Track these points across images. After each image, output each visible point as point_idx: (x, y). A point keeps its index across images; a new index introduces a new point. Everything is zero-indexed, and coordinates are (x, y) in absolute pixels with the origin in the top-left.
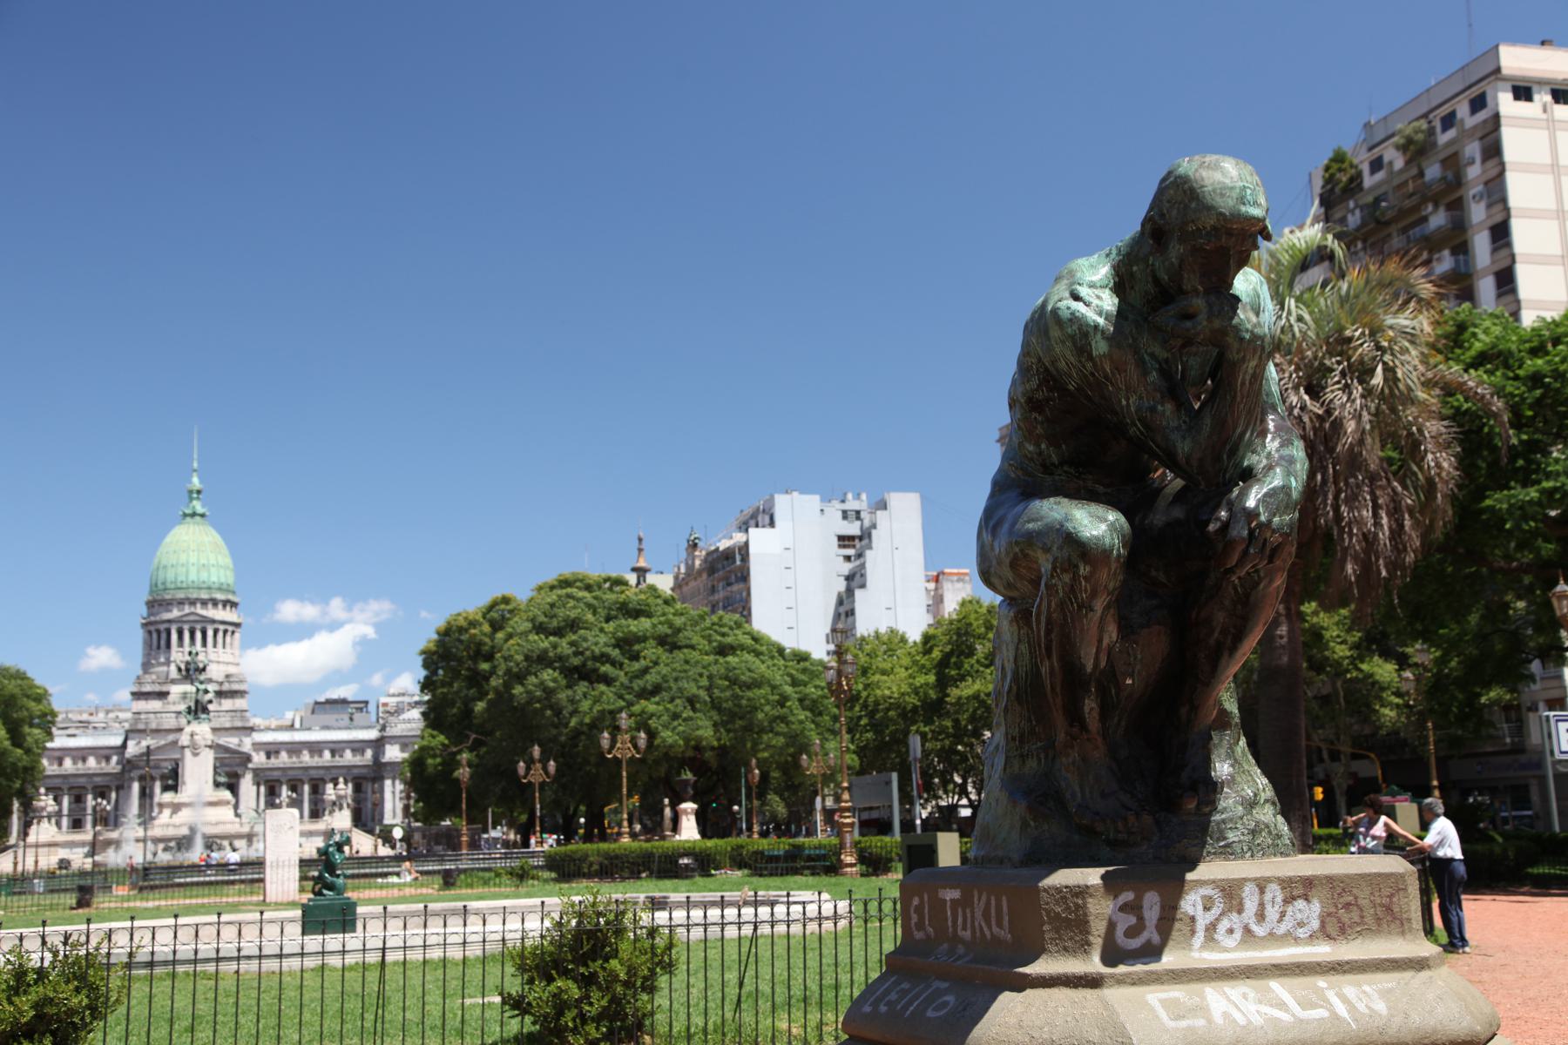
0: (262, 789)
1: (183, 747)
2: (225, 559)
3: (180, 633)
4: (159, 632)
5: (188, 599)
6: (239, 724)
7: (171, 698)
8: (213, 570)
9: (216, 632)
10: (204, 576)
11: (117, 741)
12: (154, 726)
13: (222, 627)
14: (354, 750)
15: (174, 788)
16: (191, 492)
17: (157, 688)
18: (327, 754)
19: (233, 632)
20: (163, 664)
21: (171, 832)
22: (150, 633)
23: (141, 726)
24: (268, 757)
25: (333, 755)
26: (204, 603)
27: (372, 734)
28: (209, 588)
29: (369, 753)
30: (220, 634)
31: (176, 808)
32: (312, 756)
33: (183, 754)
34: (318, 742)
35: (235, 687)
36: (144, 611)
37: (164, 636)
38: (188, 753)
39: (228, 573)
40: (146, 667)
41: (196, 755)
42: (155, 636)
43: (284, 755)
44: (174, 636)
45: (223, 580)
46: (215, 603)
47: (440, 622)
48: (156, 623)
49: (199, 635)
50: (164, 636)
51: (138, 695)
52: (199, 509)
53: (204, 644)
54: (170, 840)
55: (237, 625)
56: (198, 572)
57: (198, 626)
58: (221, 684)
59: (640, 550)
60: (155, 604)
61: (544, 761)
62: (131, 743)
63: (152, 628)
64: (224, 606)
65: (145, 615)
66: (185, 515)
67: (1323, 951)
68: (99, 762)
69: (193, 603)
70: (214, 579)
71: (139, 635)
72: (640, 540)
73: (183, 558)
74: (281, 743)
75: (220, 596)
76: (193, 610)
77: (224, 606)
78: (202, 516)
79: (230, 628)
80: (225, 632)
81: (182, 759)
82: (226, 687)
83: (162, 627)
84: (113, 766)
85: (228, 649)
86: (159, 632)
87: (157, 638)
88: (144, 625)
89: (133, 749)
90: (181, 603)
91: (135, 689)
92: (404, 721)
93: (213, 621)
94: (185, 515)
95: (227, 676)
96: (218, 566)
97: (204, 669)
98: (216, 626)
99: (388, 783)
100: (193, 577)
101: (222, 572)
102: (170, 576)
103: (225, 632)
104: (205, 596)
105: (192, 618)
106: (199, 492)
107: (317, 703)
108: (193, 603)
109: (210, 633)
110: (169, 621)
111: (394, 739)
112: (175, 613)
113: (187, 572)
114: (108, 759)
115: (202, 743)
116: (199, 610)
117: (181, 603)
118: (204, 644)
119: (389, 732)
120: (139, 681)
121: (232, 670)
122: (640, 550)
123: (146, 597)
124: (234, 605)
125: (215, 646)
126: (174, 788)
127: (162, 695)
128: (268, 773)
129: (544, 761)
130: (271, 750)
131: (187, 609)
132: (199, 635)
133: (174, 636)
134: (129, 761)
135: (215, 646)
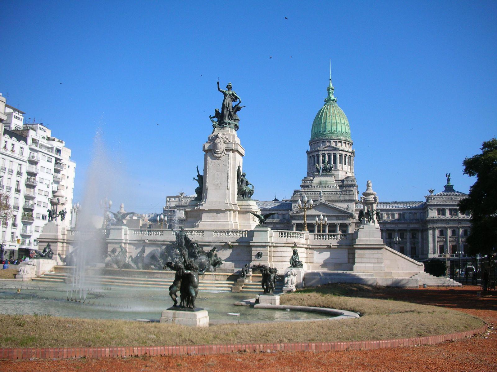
3: (324, 156)
5: (327, 139)
6: (348, 198)
8: (339, 125)
9: (341, 155)
10: (334, 128)
13: (344, 153)
22: (310, 157)
35: (350, 183)
37: (316, 158)
39: (347, 127)
42: (312, 159)
44: (321, 158)
45: (344, 130)
49: (332, 157)
50: (316, 158)
57: (332, 152)
63: (311, 155)
65: (309, 150)
70: (339, 129)
71: (305, 158)
78: (333, 100)
79: (348, 154)
86: (314, 156)
88: (308, 153)
98: (341, 152)
101: (343, 126)
109: (338, 156)
116: (333, 144)
131: (327, 144)
132: (332, 157)
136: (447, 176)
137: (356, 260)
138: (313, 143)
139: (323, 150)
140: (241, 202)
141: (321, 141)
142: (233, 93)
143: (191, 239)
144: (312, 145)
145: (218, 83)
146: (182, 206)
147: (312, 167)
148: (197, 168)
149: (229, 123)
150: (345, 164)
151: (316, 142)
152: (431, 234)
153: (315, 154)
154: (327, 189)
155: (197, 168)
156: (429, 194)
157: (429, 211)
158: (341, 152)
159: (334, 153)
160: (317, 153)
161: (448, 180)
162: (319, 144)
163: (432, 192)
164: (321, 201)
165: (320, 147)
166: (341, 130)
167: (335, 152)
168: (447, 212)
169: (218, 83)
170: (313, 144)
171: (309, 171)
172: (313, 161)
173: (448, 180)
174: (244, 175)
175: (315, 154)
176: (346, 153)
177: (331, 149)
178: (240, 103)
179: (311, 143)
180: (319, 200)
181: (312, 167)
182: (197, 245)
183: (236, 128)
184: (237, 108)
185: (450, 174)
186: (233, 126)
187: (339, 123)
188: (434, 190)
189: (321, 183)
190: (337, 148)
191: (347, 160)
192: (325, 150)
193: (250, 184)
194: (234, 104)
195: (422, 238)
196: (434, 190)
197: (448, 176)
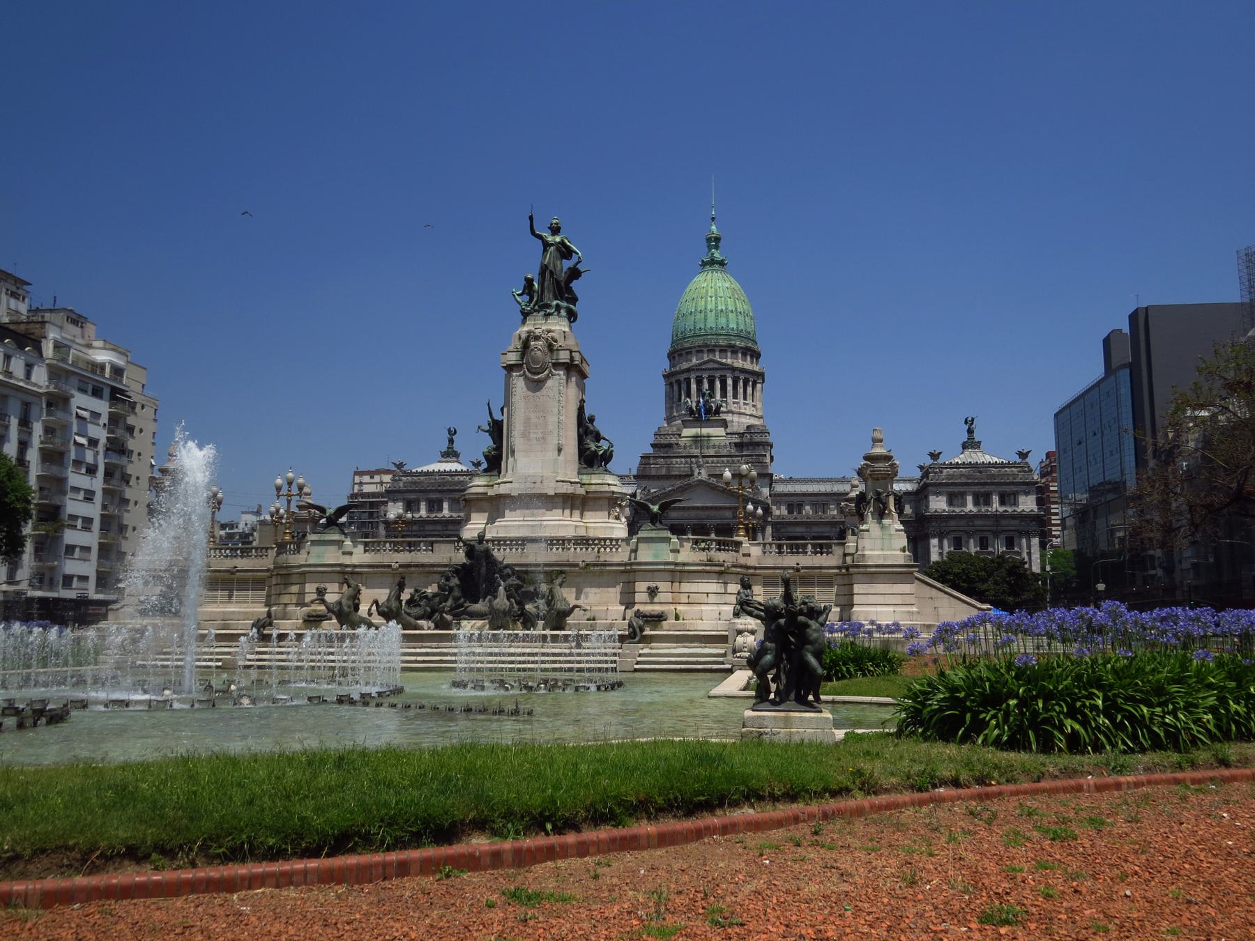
3: (699, 382)
4: (679, 382)
5: (707, 346)
10: (722, 321)
13: (742, 377)
16: (709, 240)
22: (671, 385)
26: (723, 350)
30: (741, 384)
35: (757, 438)
36: (665, 365)
37: (684, 386)
42: (676, 387)
43: (808, 509)
44: (694, 386)
45: (742, 327)
49: (718, 385)
50: (684, 386)
56: (717, 318)
58: (741, 435)
60: (675, 354)
63: (673, 380)
65: (668, 370)
70: (733, 326)
71: (661, 386)
73: (701, 304)
74: (804, 495)
76: (711, 357)
77: (744, 355)
78: (722, 263)
82: (747, 438)
85: (749, 401)
87: (676, 383)
88: (666, 377)
93: (733, 369)
94: (704, 264)
96: (738, 313)
100: (711, 323)
101: (741, 318)
104: (722, 342)
105: (711, 365)
106: (717, 239)
108: (711, 351)
109: (730, 382)
110: (688, 370)
113: (706, 319)
119: (932, 478)
123: (667, 348)
125: (735, 396)
128: (790, 529)
132: (718, 385)
135: (735, 396)
136: (966, 422)
137: (857, 599)
138: (676, 355)
139: (698, 370)
140: (586, 479)
141: (694, 350)
142: (562, 241)
143: (501, 560)
144: (674, 358)
145: (531, 218)
146: (398, 492)
147: (675, 405)
148: (488, 404)
149: (557, 306)
150: (745, 398)
151: (683, 352)
152: (934, 546)
153: (682, 377)
154: (711, 452)
155: (488, 404)
156: (928, 461)
158: (737, 374)
159: (721, 376)
160: (685, 376)
161: (970, 431)
162: (689, 356)
163: (934, 456)
164: (700, 477)
165: (726, 358)
166: (735, 327)
167: (723, 373)
168: (995, 499)
169: (531, 218)
170: (677, 357)
171: (668, 414)
172: (676, 394)
173: (970, 431)
174: (592, 420)
175: (682, 377)
176: (747, 376)
177: (716, 366)
178: (579, 262)
179: (671, 356)
180: (696, 474)
181: (675, 405)
182: (513, 570)
183: (572, 316)
184: (575, 274)
185: (973, 419)
186: (563, 312)
187: (732, 311)
188: (940, 453)
189: (697, 439)
190: (728, 365)
191: (749, 390)
192: (701, 370)
193: (604, 439)
194: (567, 264)
196: (940, 453)
197: (969, 422)
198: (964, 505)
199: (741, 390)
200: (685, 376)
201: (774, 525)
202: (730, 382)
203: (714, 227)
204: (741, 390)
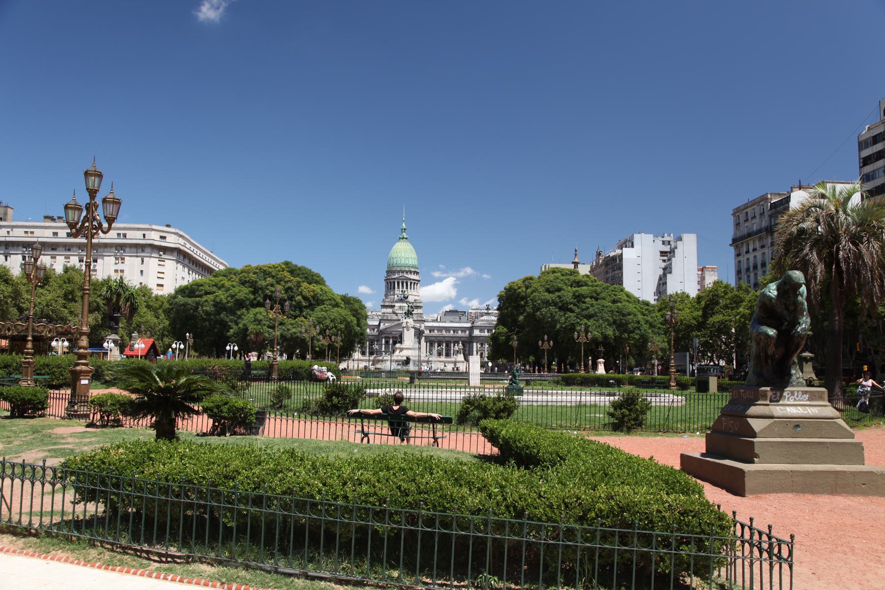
0: (428, 344)
1: (404, 327)
2: (414, 255)
4: (391, 283)
6: (420, 319)
7: (395, 308)
9: (411, 283)
10: (407, 262)
11: (377, 323)
12: (389, 318)
13: (413, 282)
14: (461, 331)
15: (401, 342)
16: (402, 229)
17: (390, 304)
18: (452, 332)
19: (417, 284)
20: (392, 295)
21: (400, 358)
22: (388, 283)
23: (385, 318)
24: (430, 332)
25: (454, 333)
26: (407, 272)
27: (469, 325)
28: (409, 266)
29: (467, 332)
31: (401, 350)
32: (446, 333)
33: (403, 330)
34: (449, 327)
35: (418, 305)
37: (392, 284)
38: (405, 329)
40: (386, 296)
41: (408, 330)
42: (389, 284)
44: (396, 285)
45: (414, 263)
46: (411, 272)
47: (506, 284)
48: (390, 279)
49: (405, 284)
50: (392, 284)
51: (383, 306)
52: (405, 236)
53: (407, 288)
54: (400, 361)
55: (419, 281)
57: (405, 281)
59: (576, 255)
60: (390, 272)
61: (548, 341)
62: (382, 324)
63: (388, 281)
64: (414, 274)
66: (400, 238)
67: (808, 403)
68: (370, 331)
69: (403, 272)
71: (384, 283)
72: (576, 251)
75: (413, 270)
77: (414, 274)
78: (406, 238)
79: (416, 282)
80: (414, 283)
81: (403, 331)
82: (415, 304)
83: (392, 281)
84: (375, 332)
86: (391, 283)
87: (390, 285)
89: (382, 326)
90: (399, 272)
91: (382, 304)
92: (481, 321)
93: (410, 279)
94: (400, 238)
95: (415, 300)
97: (407, 297)
99: (475, 344)
100: (403, 262)
102: (395, 261)
103: (414, 283)
104: (407, 269)
105: (402, 278)
106: (405, 229)
107: (446, 312)
108: (403, 272)
109: (409, 284)
110: (394, 279)
111: (477, 327)
112: (397, 276)
114: (374, 330)
115: (410, 326)
117: (399, 272)
118: (407, 288)
119: (475, 324)
120: (384, 301)
121: (417, 298)
122: (576, 255)
123: (386, 269)
124: (417, 273)
125: (411, 289)
126: (401, 342)
127: (393, 307)
129: (548, 341)
130: (431, 329)
132: (405, 284)
133: (396, 285)
134: (381, 331)
135: (411, 289)
157: (475, 330)
160: (393, 280)
179: (388, 272)
195: (469, 347)
198: (484, 332)
199: (412, 287)
200: (393, 280)
201: (425, 337)
202: (409, 284)
203: (404, 225)
204: (412, 287)
